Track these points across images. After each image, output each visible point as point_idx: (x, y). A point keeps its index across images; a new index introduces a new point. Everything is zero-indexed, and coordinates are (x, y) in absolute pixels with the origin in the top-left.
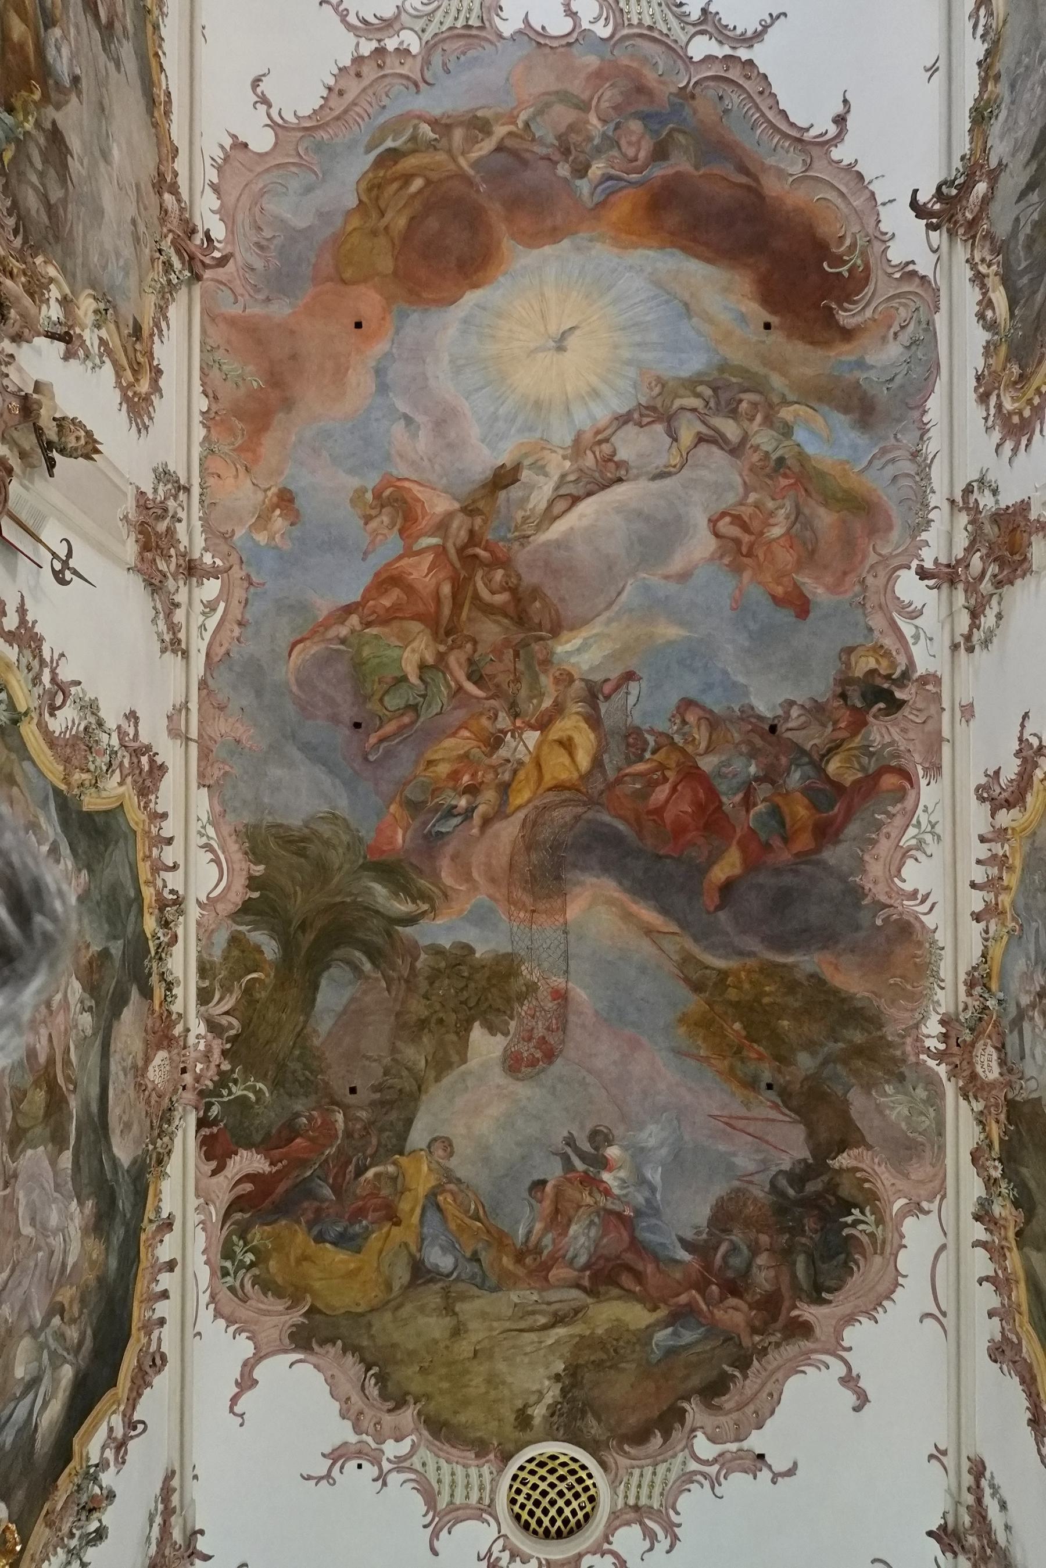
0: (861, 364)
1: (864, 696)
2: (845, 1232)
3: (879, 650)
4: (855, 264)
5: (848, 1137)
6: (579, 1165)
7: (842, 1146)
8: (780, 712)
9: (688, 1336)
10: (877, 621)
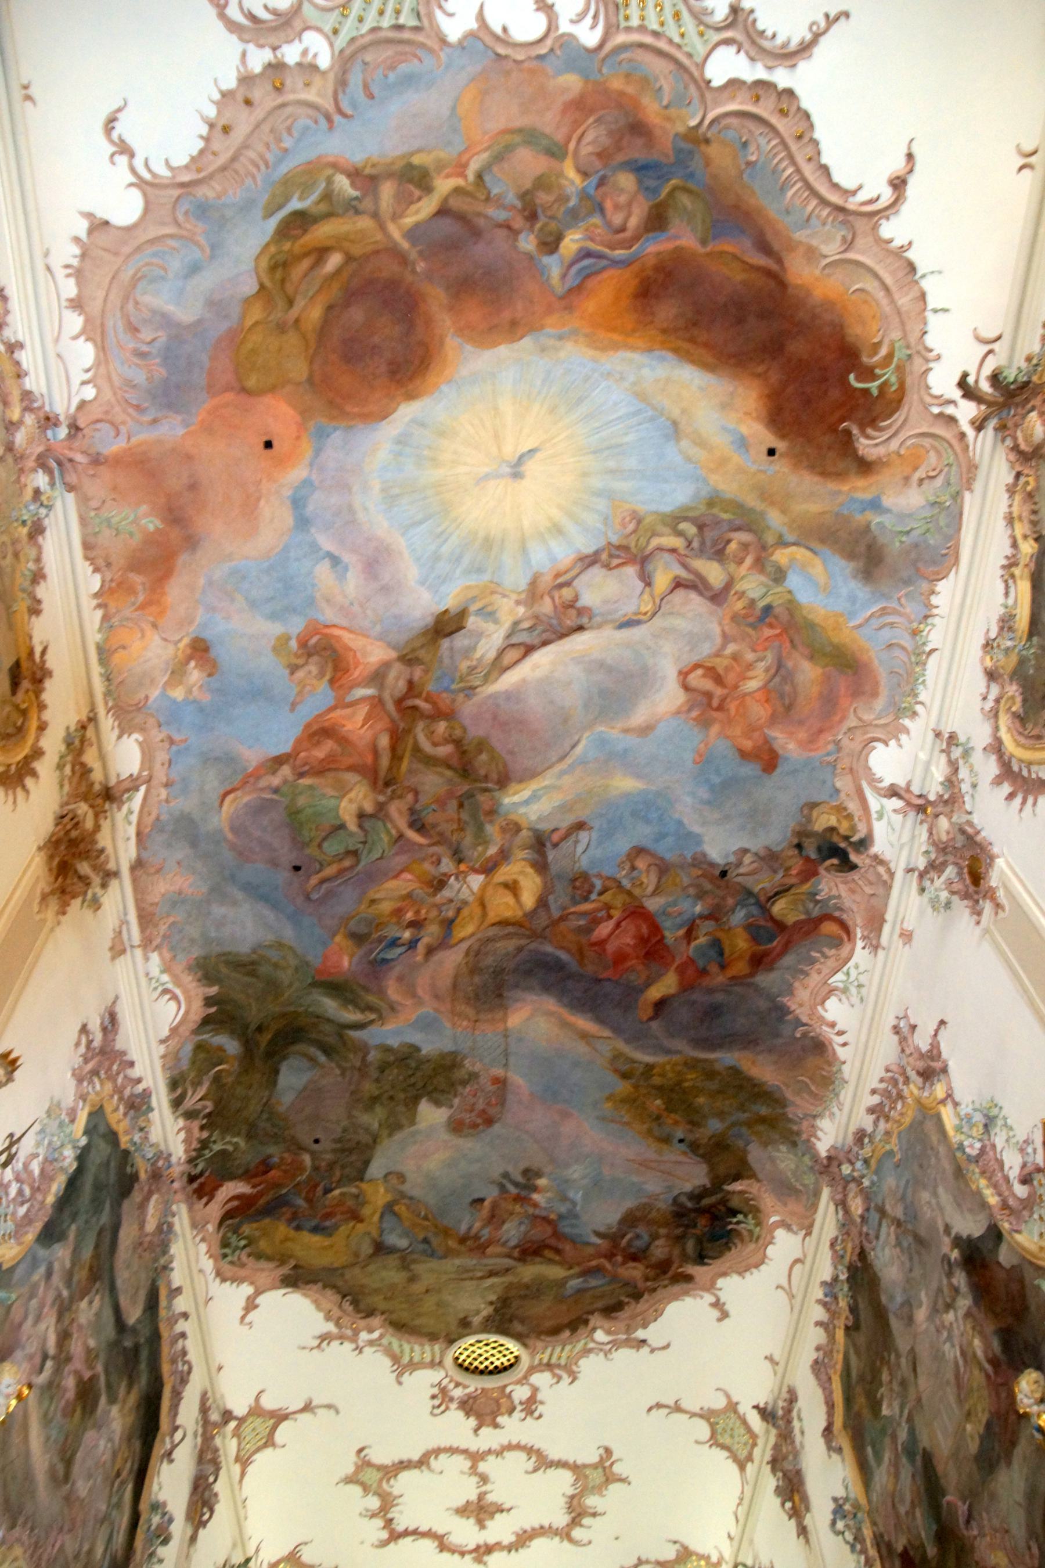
0: (875, 505)
1: (819, 849)
2: (730, 1227)
3: (840, 809)
4: (885, 383)
5: (742, 1171)
6: (513, 1190)
7: (737, 1177)
8: (732, 859)
9: (593, 1282)
10: (843, 783)
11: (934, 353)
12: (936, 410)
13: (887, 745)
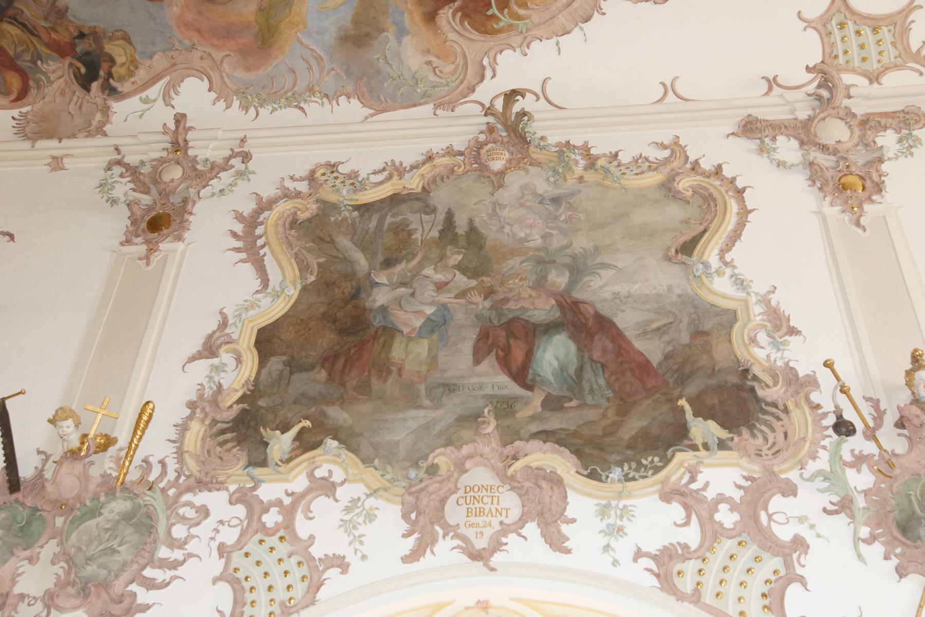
0: (402, 32)
1: (88, 53)
3: (133, 65)
4: (498, 19)
10: (160, 61)
11: (527, 51)
12: (485, 62)
13: (210, 90)
